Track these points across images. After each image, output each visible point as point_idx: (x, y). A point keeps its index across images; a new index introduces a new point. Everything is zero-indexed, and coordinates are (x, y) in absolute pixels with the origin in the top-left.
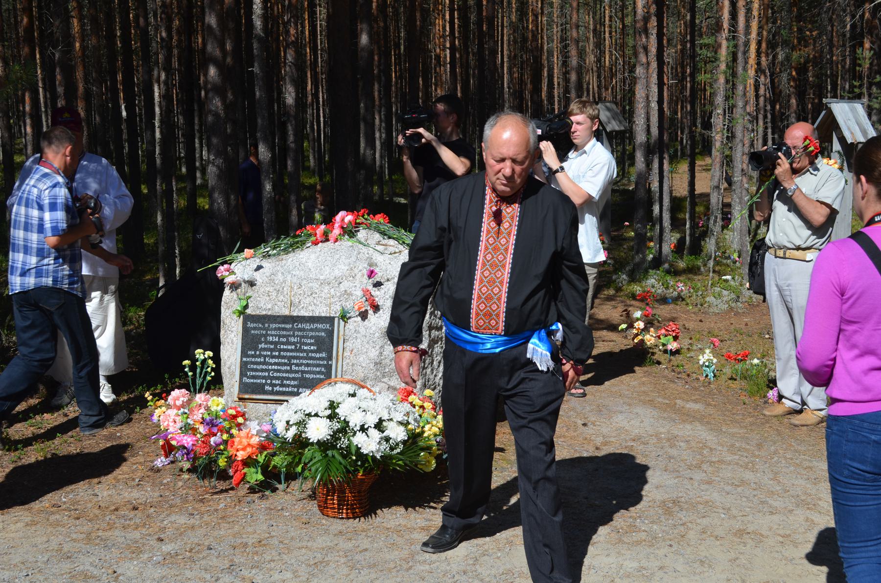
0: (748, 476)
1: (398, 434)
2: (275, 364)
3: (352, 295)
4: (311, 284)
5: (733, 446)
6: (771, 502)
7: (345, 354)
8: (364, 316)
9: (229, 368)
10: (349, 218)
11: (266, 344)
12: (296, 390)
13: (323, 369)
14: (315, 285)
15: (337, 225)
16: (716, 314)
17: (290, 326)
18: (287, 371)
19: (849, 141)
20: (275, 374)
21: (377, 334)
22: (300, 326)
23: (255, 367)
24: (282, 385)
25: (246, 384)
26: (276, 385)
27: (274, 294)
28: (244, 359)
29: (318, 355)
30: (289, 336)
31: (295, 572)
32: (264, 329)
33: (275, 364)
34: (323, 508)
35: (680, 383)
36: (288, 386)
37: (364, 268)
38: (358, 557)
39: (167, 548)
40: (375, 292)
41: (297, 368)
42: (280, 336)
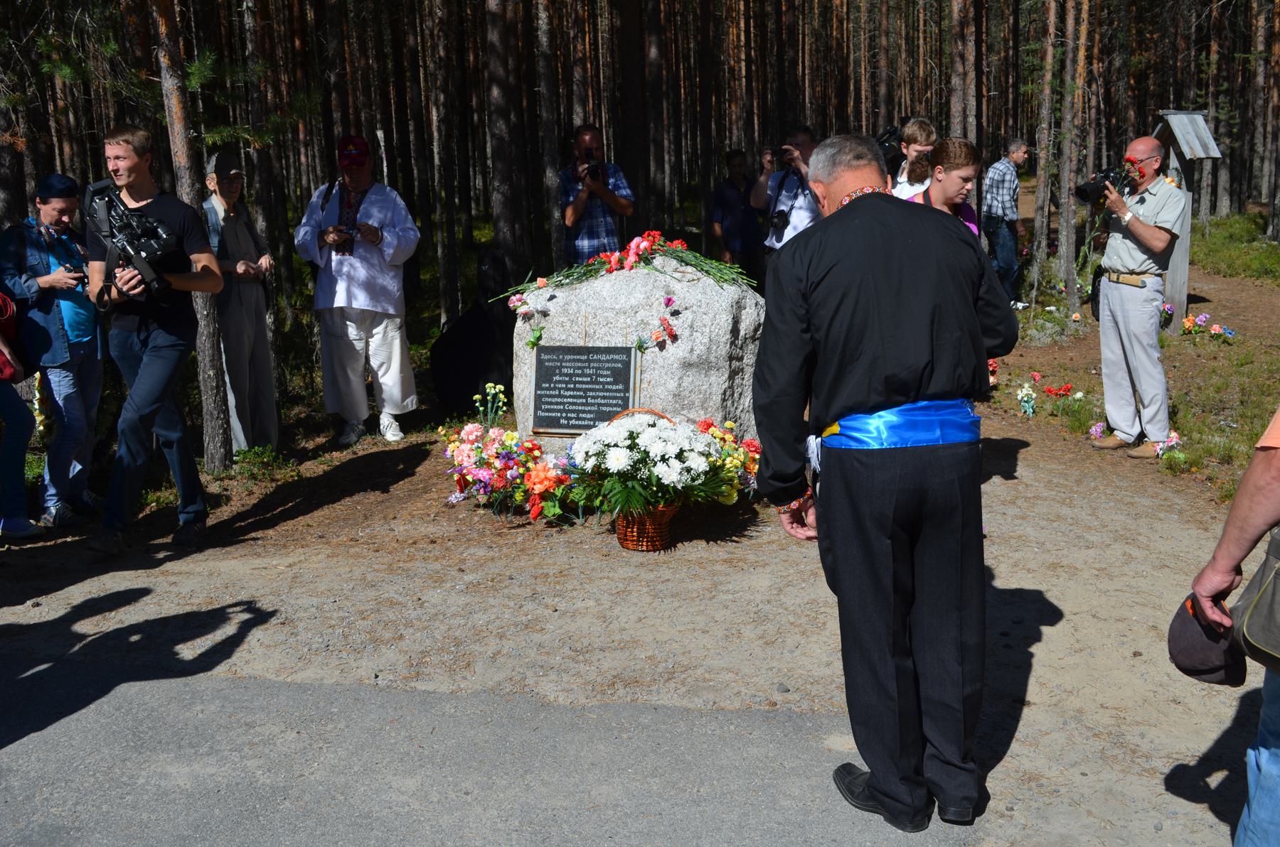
0: (1065, 511)
1: (699, 464)
2: (570, 397)
5: (1049, 482)
6: (1087, 536)
7: (644, 385)
8: (662, 346)
10: (644, 244)
14: (610, 314)
15: (632, 252)
16: (1038, 348)
18: (582, 404)
19: (1188, 157)
24: (578, 419)
26: (571, 419)
27: (568, 324)
31: (597, 600)
32: (558, 360)
33: (570, 397)
34: (623, 541)
35: (996, 419)
36: (584, 419)
37: (660, 296)
38: (660, 587)
39: (468, 578)
40: (673, 321)
42: (575, 368)
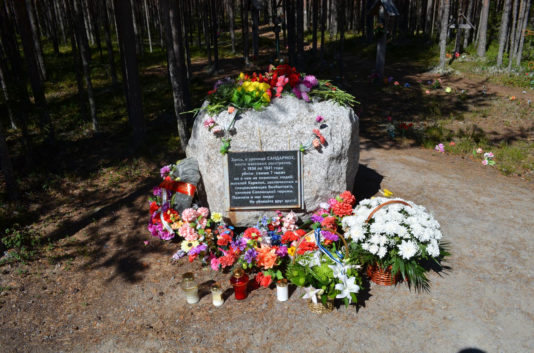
2: (255, 185)
3: (304, 134)
7: (306, 174)
9: (219, 189)
11: (247, 172)
12: (272, 201)
13: (291, 187)
17: (265, 159)
18: (265, 190)
20: (256, 192)
22: (271, 158)
23: (240, 188)
24: (262, 199)
25: (235, 200)
26: (257, 200)
27: (248, 136)
28: (232, 184)
29: (287, 178)
30: (264, 166)
32: (245, 162)
33: (255, 185)
36: (267, 199)
42: (257, 167)
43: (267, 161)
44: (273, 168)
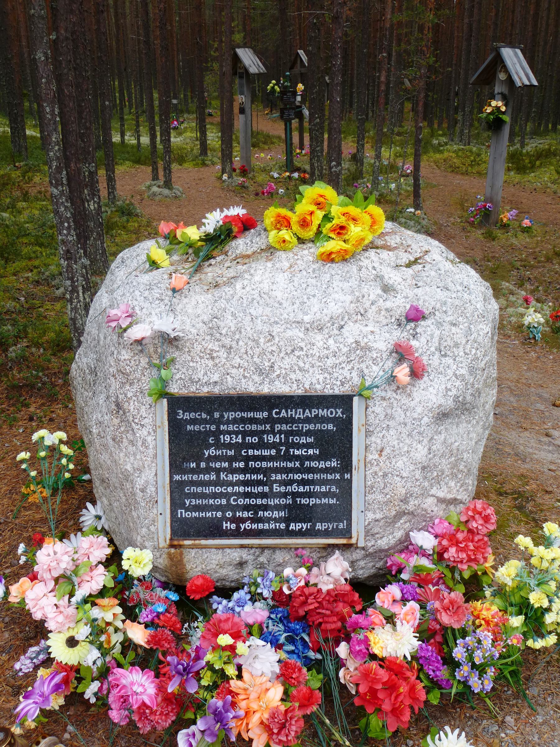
3: (370, 349)
4: (289, 333)
9: (142, 491)
12: (283, 526)
13: (334, 489)
17: (265, 414)
21: (426, 419)
22: (283, 413)
23: (199, 490)
24: (255, 520)
25: (184, 521)
26: (243, 520)
28: (177, 477)
29: (322, 465)
30: (264, 432)
32: (213, 421)
41: (283, 489)
42: (245, 434)
43: (270, 420)
44: (287, 438)
